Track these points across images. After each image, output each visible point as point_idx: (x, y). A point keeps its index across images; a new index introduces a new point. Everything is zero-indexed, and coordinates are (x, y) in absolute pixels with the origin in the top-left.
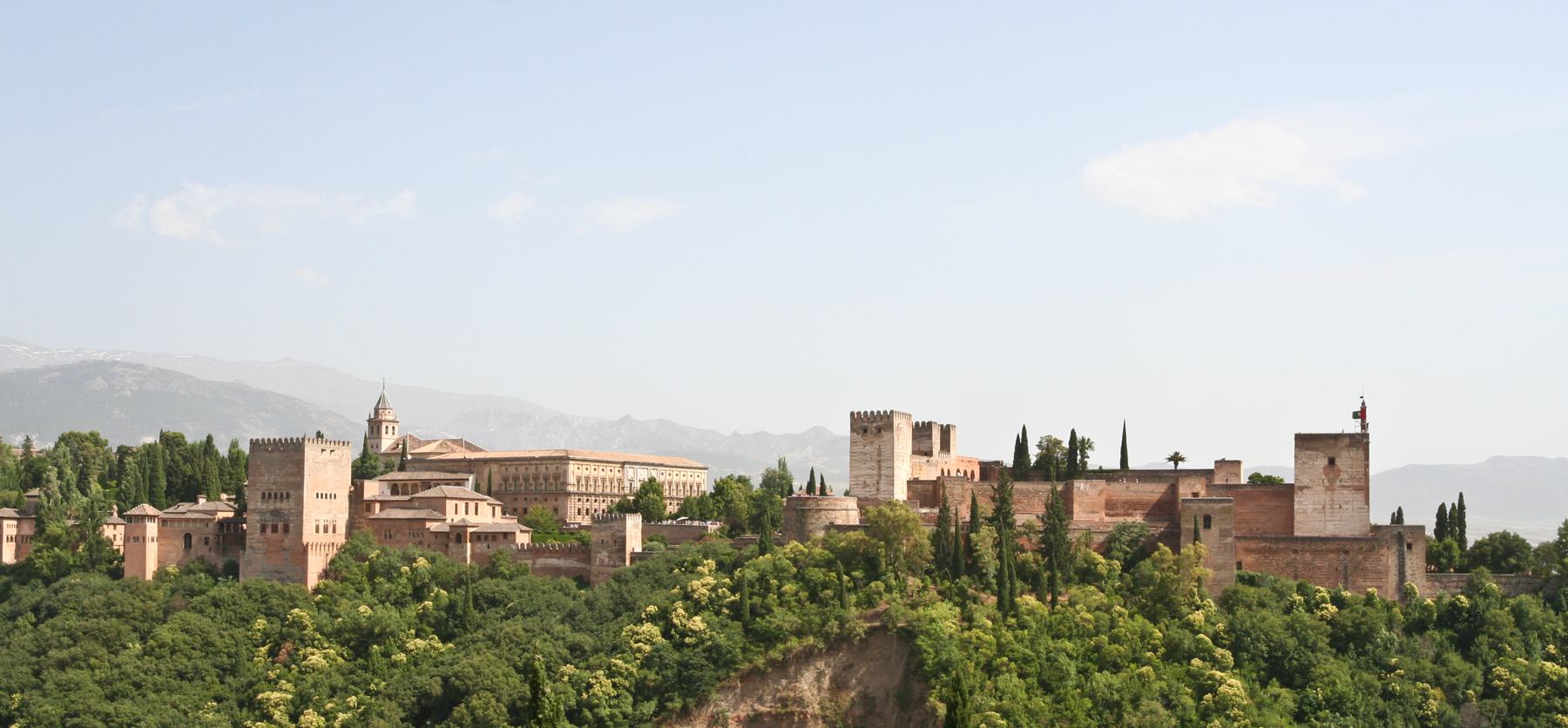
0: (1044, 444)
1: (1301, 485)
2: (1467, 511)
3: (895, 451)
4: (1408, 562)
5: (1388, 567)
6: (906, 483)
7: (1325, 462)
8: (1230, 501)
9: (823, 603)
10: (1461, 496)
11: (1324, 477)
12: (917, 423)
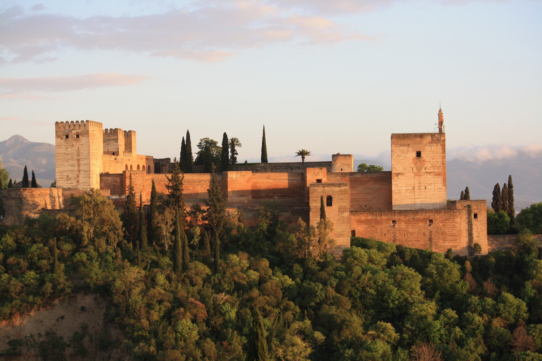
0: (204, 144)
1: (397, 172)
2: (515, 189)
3: (91, 151)
4: (474, 227)
5: (461, 231)
6: (99, 176)
7: (414, 154)
8: (345, 185)
9: (38, 269)
10: (510, 178)
11: (413, 166)
12: (106, 130)
